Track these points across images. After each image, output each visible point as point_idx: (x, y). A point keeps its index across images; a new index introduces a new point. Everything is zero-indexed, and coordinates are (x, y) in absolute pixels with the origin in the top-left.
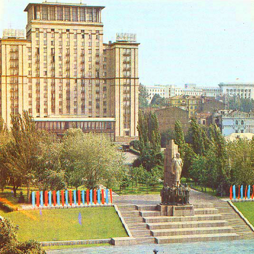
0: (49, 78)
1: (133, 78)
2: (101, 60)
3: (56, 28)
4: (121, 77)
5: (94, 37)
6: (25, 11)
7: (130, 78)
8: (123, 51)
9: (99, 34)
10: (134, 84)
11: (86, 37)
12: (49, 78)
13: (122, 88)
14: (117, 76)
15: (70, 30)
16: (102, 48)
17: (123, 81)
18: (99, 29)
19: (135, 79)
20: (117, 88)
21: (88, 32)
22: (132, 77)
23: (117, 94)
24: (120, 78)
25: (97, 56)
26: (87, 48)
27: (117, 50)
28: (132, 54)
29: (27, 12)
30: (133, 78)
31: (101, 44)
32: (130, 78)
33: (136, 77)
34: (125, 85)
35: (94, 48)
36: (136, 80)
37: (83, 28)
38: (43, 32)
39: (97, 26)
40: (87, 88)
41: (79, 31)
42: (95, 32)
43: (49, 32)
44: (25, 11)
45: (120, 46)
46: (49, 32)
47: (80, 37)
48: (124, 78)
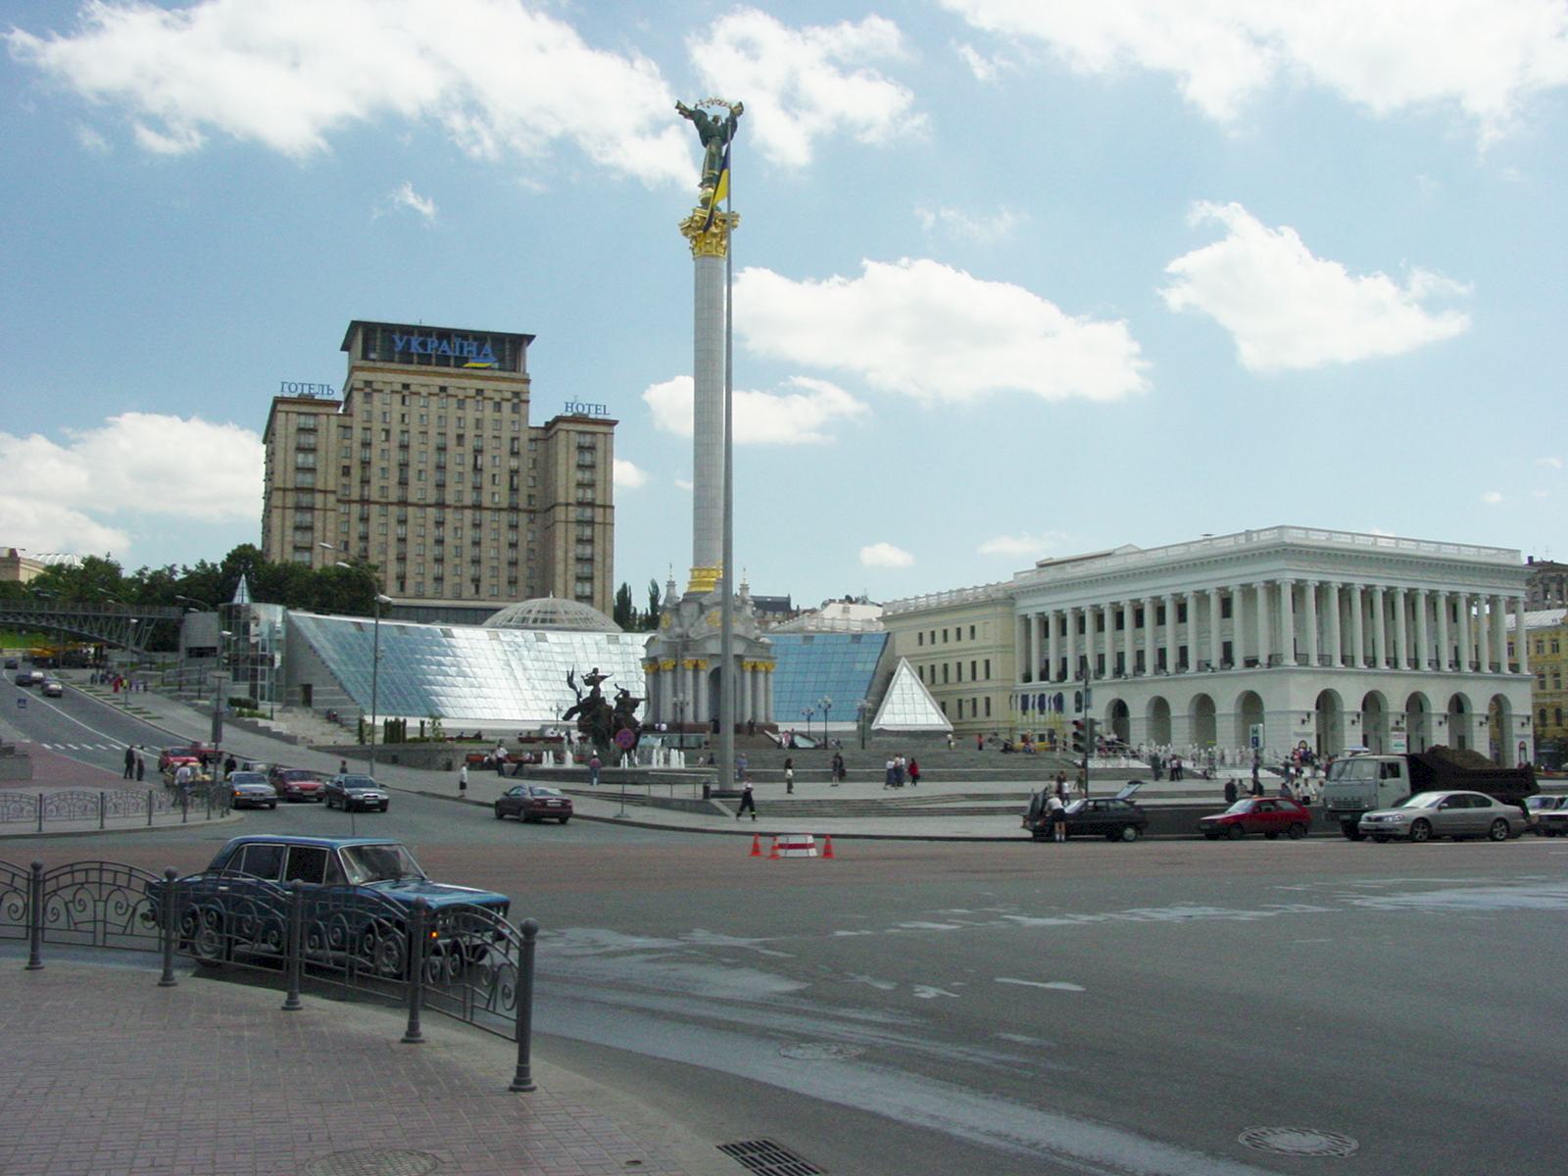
0: (392, 504)
1: (600, 506)
2: (523, 464)
3: (415, 381)
5: (506, 407)
6: (342, 349)
7: (592, 505)
8: (575, 439)
9: (519, 401)
12: (392, 504)
13: (572, 526)
16: (524, 437)
17: (574, 513)
18: (517, 387)
19: (604, 507)
20: (560, 529)
23: (560, 543)
24: (567, 505)
27: (562, 435)
28: (600, 445)
29: (346, 353)
30: (600, 506)
31: (524, 428)
32: (592, 505)
33: (608, 503)
34: (579, 522)
35: (506, 435)
37: (480, 384)
39: (513, 380)
40: (486, 534)
41: (472, 392)
42: (509, 395)
44: (342, 349)
45: (571, 427)
46: (397, 392)
48: (581, 504)
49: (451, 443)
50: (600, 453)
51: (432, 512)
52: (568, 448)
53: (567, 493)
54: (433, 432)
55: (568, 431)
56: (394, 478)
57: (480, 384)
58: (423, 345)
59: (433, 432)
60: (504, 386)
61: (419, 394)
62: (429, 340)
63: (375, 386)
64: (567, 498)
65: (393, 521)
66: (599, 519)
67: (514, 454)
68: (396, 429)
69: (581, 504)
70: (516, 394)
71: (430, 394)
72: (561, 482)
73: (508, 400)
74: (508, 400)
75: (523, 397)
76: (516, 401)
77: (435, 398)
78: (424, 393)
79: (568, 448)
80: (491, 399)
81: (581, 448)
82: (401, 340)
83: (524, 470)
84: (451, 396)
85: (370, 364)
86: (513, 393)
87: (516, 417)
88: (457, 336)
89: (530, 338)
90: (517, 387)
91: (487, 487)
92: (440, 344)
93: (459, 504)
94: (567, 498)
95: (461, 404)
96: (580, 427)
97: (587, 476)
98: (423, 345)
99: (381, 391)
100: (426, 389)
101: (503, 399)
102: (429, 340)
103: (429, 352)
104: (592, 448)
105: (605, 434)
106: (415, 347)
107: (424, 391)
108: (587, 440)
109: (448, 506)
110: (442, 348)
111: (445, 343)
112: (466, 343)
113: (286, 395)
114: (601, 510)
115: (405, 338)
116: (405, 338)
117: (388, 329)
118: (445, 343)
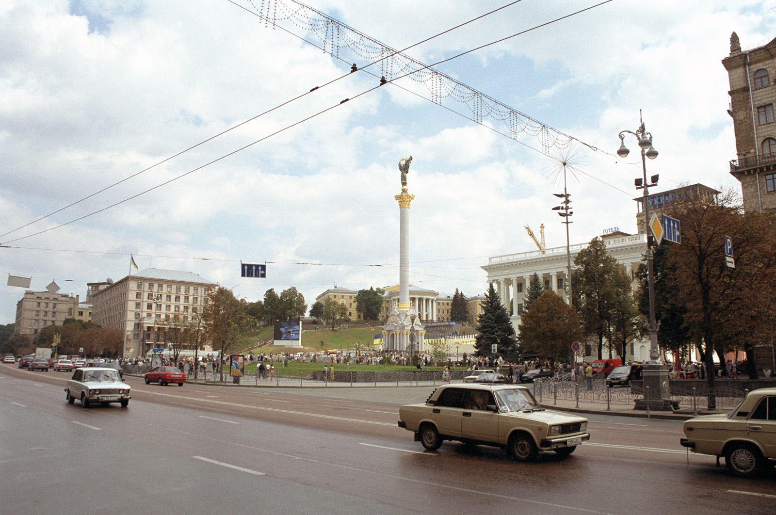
58: (659, 200)
62: (661, 198)
82: (651, 201)
88: (671, 193)
92: (665, 198)
98: (659, 200)
102: (661, 198)
103: (661, 202)
106: (656, 202)
110: (666, 200)
111: (667, 197)
112: (674, 195)
113: (605, 234)
115: (652, 200)
116: (652, 200)
118: (667, 197)
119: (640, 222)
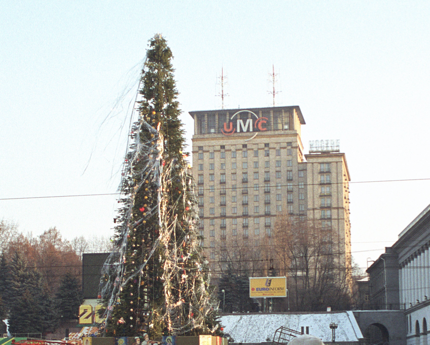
0: (216, 218)
1: (334, 208)
4: (316, 206)
7: (329, 208)
10: (336, 217)
11: (272, 153)
12: (216, 218)
14: (310, 206)
15: (248, 145)
18: (289, 139)
19: (338, 208)
21: (275, 146)
22: (334, 205)
24: (314, 209)
25: (290, 180)
26: (272, 170)
28: (334, 170)
30: (334, 208)
32: (329, 208)
33: (340, 206)
35: (284, 170)
36: (340, 210)
37: (266, 140)
38: (208, 151)
39: (287, 135)
42: (285, 145)
43: (217, 151)
45: (315, 160)
46: (217, 151)
47: (261, 153)
48: (322, 208)
49: (251, 177)
50: (334, 175)
51: (218, 222)
52: (313, 174)
53: (314, 202)
54: (239, 172)
55: (313, 163)
56: (218, 200)
57: (266, 140)
59: (239, 172)
60: (281, 139)
61: (230, 150)
63: (204, 149)
64: (314, 205)
65: (217, 228)
66: (335, 216)
67: (290, 180)
68: (217, 172)
69: (322, 208)
70: (289, 144)
71: (259, 149)
72: (310, 195)
73: (284, 148)
74: (284, 148)
75: (294, 145)
76: (289, 147)
77: (240, 152)
78: (233, 148)
79: (313, 174)
80: (274, 148)
81: (321, 173)
83: (295, 189)
84: (249, 149)
85: (202, 136)
86: (287, 143)
87: (290, 158)
89: (297, 108)
90: (289, 139)
91: (273, 202)
93: (256, 214)
94: (314, 205)
95: (256, 154)
96: (320, 160)
97: (326, 190)
99: (208, 151)
100: (234, 146)
101: (281, 148)
104: (329, 172)
105: (337, 162)
107: (233, 148)
108: (325, 167)
109: (250, 217)
114: (336, 211)
117: (211, 114)
119: (197, 149)
